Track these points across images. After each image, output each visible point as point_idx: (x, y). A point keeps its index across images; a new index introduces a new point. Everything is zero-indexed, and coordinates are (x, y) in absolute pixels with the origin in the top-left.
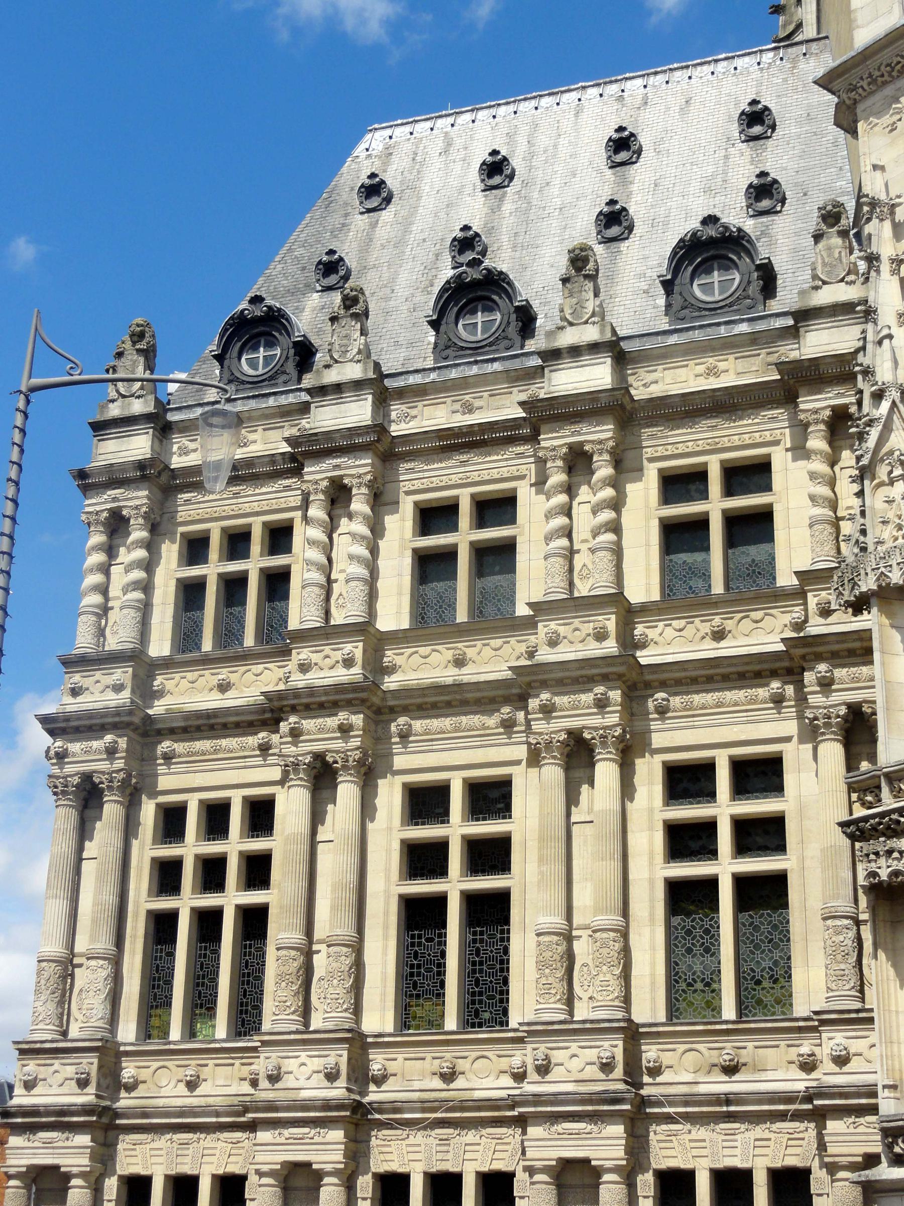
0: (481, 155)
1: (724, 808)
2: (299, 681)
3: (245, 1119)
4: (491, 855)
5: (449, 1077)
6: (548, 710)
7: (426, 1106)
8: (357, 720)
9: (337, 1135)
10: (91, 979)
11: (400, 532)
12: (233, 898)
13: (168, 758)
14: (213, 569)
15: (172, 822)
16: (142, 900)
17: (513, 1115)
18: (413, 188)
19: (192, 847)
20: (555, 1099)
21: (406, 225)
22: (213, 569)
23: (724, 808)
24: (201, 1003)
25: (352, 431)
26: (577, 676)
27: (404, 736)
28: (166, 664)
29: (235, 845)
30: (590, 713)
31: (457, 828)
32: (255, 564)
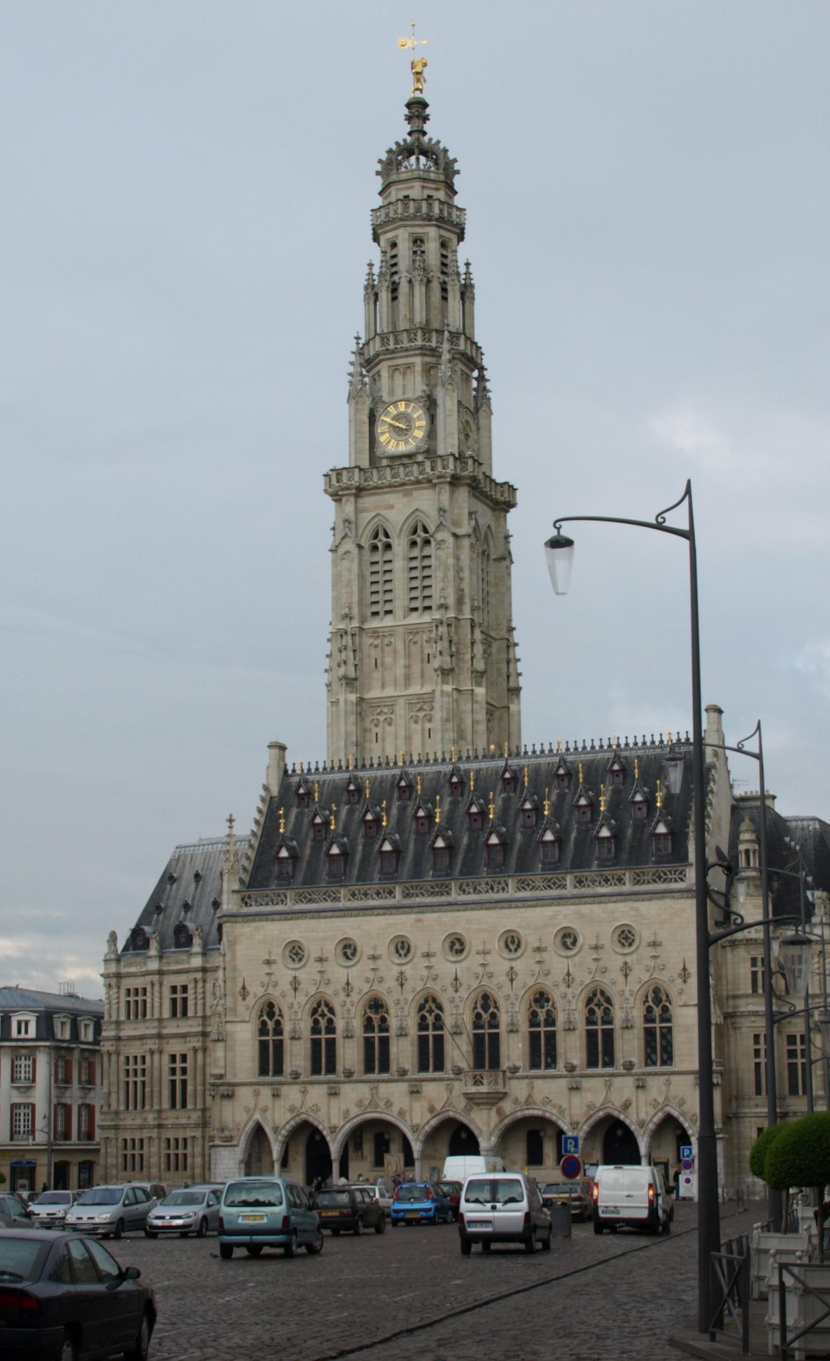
3: (141, 1128)
4: (184, 1071)
5: (177, 1118)
6: (190, 1042)
9: (156, 1130)
10: (114, 1097)
11: (167, 994)
12: (139, 1079)
14: (132, 999)
17: (184, 1127)
18: (181, 876)
19: (131, 1067)
21: (178, 890)
22: (132, 999)
26: (194, 1034)
30: (197, 1043)
31: (179, 1065)
32: (140, 998)
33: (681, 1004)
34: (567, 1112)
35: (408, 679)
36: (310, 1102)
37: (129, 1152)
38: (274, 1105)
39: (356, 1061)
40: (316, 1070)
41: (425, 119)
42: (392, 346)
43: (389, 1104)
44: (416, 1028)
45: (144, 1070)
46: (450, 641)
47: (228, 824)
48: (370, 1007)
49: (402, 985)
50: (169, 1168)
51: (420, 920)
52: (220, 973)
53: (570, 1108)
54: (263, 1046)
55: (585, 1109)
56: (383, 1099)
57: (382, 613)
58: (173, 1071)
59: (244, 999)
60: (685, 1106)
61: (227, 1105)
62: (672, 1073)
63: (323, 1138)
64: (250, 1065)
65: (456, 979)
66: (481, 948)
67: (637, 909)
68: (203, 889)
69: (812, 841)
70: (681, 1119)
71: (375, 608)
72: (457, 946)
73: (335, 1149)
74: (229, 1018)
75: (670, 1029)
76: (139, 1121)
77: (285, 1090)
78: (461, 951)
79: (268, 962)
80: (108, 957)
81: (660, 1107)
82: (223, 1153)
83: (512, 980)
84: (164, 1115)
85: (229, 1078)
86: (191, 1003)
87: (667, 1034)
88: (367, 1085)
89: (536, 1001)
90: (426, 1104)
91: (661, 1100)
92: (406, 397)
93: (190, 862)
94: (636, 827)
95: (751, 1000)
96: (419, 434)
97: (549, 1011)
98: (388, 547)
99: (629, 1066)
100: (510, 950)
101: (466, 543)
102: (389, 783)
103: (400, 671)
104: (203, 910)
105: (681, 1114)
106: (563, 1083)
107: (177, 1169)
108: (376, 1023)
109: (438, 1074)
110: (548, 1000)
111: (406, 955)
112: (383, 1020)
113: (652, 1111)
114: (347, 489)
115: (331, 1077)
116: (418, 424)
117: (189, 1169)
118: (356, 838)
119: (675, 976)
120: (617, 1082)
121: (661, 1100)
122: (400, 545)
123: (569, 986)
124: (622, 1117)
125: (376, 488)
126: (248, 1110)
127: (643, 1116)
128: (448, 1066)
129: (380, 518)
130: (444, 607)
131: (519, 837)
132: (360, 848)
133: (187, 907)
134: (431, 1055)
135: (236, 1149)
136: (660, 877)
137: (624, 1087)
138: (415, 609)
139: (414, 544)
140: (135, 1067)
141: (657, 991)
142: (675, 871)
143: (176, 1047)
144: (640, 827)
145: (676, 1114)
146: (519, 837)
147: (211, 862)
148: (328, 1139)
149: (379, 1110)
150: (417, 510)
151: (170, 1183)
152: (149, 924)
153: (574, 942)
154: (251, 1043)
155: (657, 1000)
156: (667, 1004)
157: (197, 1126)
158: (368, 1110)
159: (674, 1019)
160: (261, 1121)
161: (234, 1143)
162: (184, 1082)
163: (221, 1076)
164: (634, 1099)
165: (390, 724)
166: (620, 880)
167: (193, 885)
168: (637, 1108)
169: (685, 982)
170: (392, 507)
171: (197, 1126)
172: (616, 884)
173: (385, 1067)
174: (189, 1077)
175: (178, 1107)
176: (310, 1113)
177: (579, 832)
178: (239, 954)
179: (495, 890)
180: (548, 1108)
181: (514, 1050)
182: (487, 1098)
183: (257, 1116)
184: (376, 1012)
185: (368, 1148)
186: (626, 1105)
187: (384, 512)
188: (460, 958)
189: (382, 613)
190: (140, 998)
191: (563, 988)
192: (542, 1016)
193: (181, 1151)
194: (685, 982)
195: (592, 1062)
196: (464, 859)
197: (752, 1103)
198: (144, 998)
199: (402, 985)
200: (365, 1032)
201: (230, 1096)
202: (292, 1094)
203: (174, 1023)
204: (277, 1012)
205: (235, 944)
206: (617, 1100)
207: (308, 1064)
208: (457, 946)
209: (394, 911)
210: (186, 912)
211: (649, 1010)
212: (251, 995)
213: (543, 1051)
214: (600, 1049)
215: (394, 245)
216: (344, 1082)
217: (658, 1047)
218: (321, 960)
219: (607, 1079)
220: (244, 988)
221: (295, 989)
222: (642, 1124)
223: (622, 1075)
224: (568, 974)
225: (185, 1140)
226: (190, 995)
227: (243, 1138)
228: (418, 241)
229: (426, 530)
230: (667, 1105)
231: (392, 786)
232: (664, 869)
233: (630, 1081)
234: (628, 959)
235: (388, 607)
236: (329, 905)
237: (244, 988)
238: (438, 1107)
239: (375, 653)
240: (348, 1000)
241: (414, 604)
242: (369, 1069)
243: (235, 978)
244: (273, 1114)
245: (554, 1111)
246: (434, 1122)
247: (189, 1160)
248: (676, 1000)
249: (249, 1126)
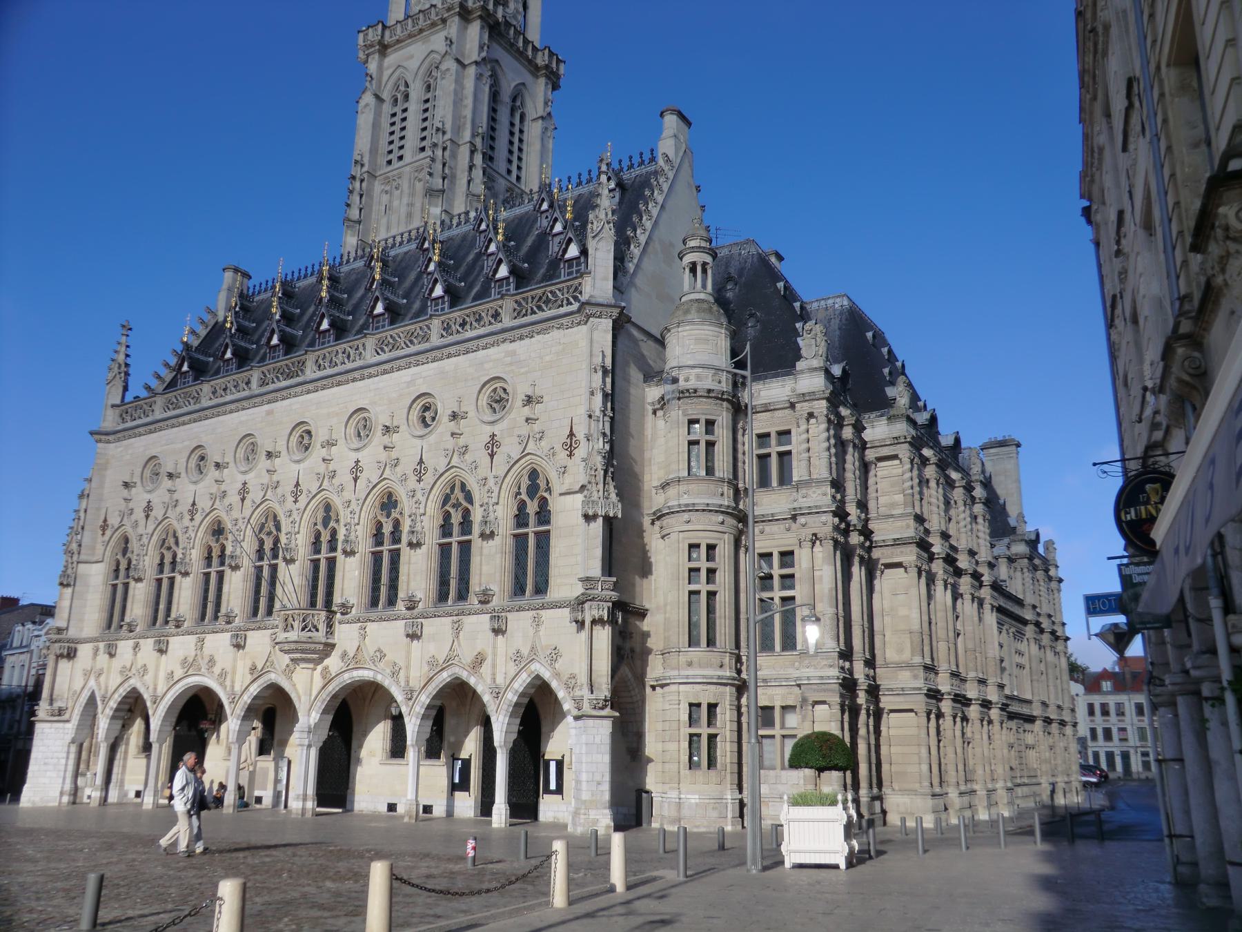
34: (402, 674)
35: (410, 216)
38: (109, 668)
43: (212, 662)
46: (444, 165)
53: (408, 667)
55: (426, 668)
60: (560, 660)
61: (64, 665)
62: (543, 607)
67: (513, 353)
69: (838, 321)
70: (554, 685)
74: (83, 557)
82: (47, 731)
85: (72, 633)
87: (543, 540)
90: (249, 664)
91: (525, 651)
95: (683, 488)
101: (472, 71)
103: (403, 210)
106: (399, 627)
113: (513, 669)
114: (372, 46)
119: (558, 447)
120: (469, 621)
121: (525, 651)
123: (419, 481)
124: (472, 681)
129: (401, 70)
135: (68, 725)
136: (547, 302)
141: (534, 475)
142: (569, 288)
145: (546, 675)
154: (101, 588)
156: (546, 495)
161: (66, 717)
164: (489, 652)
166: (496, 315)
168: (494, 666)
169: (570, 455)
181: (351, 579)
182: (303, 651)
186: (479, 661)
191: (412, 482)
192: (387, 529)
194: (570, 455)
197: (683, 659)
201: (71, 655)
205: (106, 469)
206: (467, 656)
209: (245, 403)
211: (522, 506)
218: (170, 476)
219: (455, 618)
232: (553, 288)
234: (496, 429)
237: (105, 521)
239: (385, 198)
243: (98, 509)
244: (107, 678)
248: (557, 487)
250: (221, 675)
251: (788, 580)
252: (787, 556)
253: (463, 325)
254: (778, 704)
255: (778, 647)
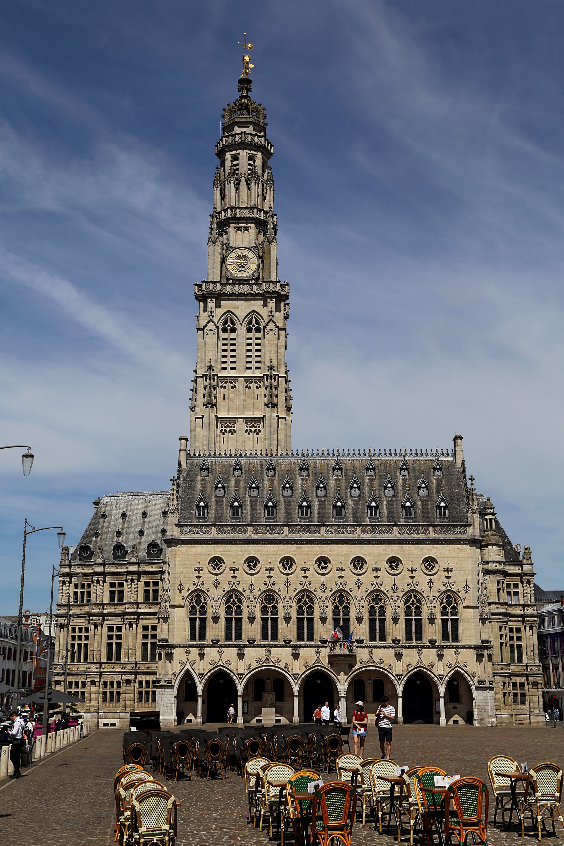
0: (121, 512)
1: (150, 632)
2: (93, 611)
4: (119, 637)
7: (110, 672)
8: (101, 618)
12: (83, 642)
13: (73, 620)
14: (79, 590)
15: (74, 630)
16: (70, 642)
19: (77, 634)
20: (126, 672)
21: (109, 523)
22: (79, 590)
23: (150, 632)
24: (79, 660)
25: (100, 573)
27: (107, 620)
28: (72, 605)
29: (83, 634)
31: (115, 633)
32: (85, 590)
33: (464, 606)
36: (224, 658)
37: (108, 690)
39: (256, 633)
40: (228, 638)
41: (249, 90)
42: (238, 216)
43: (278, 661)
44: (296, 613)
45: (87, 638)
47: (172, 482)
48: (266, 599)
49: (287, 587)
50: (105, 700)
51: (301, 548)
52: (167, 574)
54: (193, 621)
56: (273, 657)
57: (228, 368)
58: (110, 637)
59: (181, 592)
63: (233, 681)
64: (184, 633)
65: (323, 585)
66: (339, 566)
68: (128, 525)
71: (224, 365)
72: (323, 564)
73: (240, 689)
74: (171, 603)
75: (457, 620)
76: (82, 669)
77: (207, 650)
78: (325, 568)
79: (199, 570)
80: (63, 563)
81: (453, 667)
83: (359, 587)
84: (103, 666)
85: (171, 642)
86: (126, 594)
87: (455, 622)
88: (264, 649)
89: (373, 599)
91: (453, 664)
92: (244, 246)
93: (116, 507)
94: (422, 501)
96: (254, 267)
97: (382, 607)
98: (233, 330)
99: (432, 642)
100: (357, 569)
102: (259, 466)
104: (131, 536)
105: (466, 672)
107: (112, 701)
108: (269, 610)
109: (310, 643)
110: (381, 600)
111: (289, 569)
112: (274, 607)
113: (448, 670)
115: (239, 643)
116: (253, 262)
117: (123, 703)
118: (245, 497)
119: (461, 589)
122: (241, 329)
125: (228, 295)
126: (181, 663)
127: (441, 673)
128: (317, 637)
130: (271, 368)
131: (350, 502)
132: (249, 503)
133: (119, 534)
134: (305, 629)
137: (430, 655)
138: (250, 368)
139: (249, 330)
140: (80, 634)
143: (115, 622)
144: (424, 502)
146: (350, 502)
147: (132, 507)
148: (237, 682)
149: (272, 664)
150: (254, 311)
151: (105, 711)
152: (90, 543)
153: (397, 566)
154: (185, 619)
155: (449, 603)
157: (131, 673)
158: (264, 664)
159: (459, 614)
160: (191, 669)
162: (119, 645)
163: (167, 641)
165: (232, 434)
167: (121, 521)
170: (237, 307)
171: (131, 673)
172: (424, 533)
173: (275, 637)
174: (123, 641)
175: (113, 661)
176: (226, 666)
177: (388, 502)
178: (177, 563)
179: (348, 532)
180: (382, 666)
183: (188, 667)
184: (269, 603)
185: (251, 688)
186: (432, 665)
187: (232, 310)
188: (325, 572)
189: (228, 368)
190: (85, 590)
193: (115, 690)
194: (467, 593)
195: (409, 638)
196: (318, 513)
198: (89, 590)
199: (287, 587)
200: (262, 615)
202: (212, 654)
203: (114, 607)
204: (203, 601)
207: (224, 634)
208: (323, 564)
210: (118, 537)
212: (186, 589)
213: (377, 630)
214: (414, 631)
215: (235, 158)
216: (248, 647)
217: (450, 630)
220: (181, 585)
221: (216, 587)
222: (441, 677)
223: (429, 648)
224: (395, 585)
225: (119, 683)
226: (126, 588)
227: (177, 681)
228: (251, 158)
229: (257, 323)
230: (458, 666)
231: (262, 467)
233: (434, 651)
235: (233, 365)
236: (240, 537)
237: (181, 585)
238: (311, 663)
240: (252, 595)
241: (249, 365)
242: (264, 637)
245: (386, 668)
246: (307, 673)
247: (123, 695)
249: (182, 673)
250: (286, 667)
251: (519, 639)
252: (518, 630)
253: (410, 530)
254: (518, 682)
255: (516, 662)
